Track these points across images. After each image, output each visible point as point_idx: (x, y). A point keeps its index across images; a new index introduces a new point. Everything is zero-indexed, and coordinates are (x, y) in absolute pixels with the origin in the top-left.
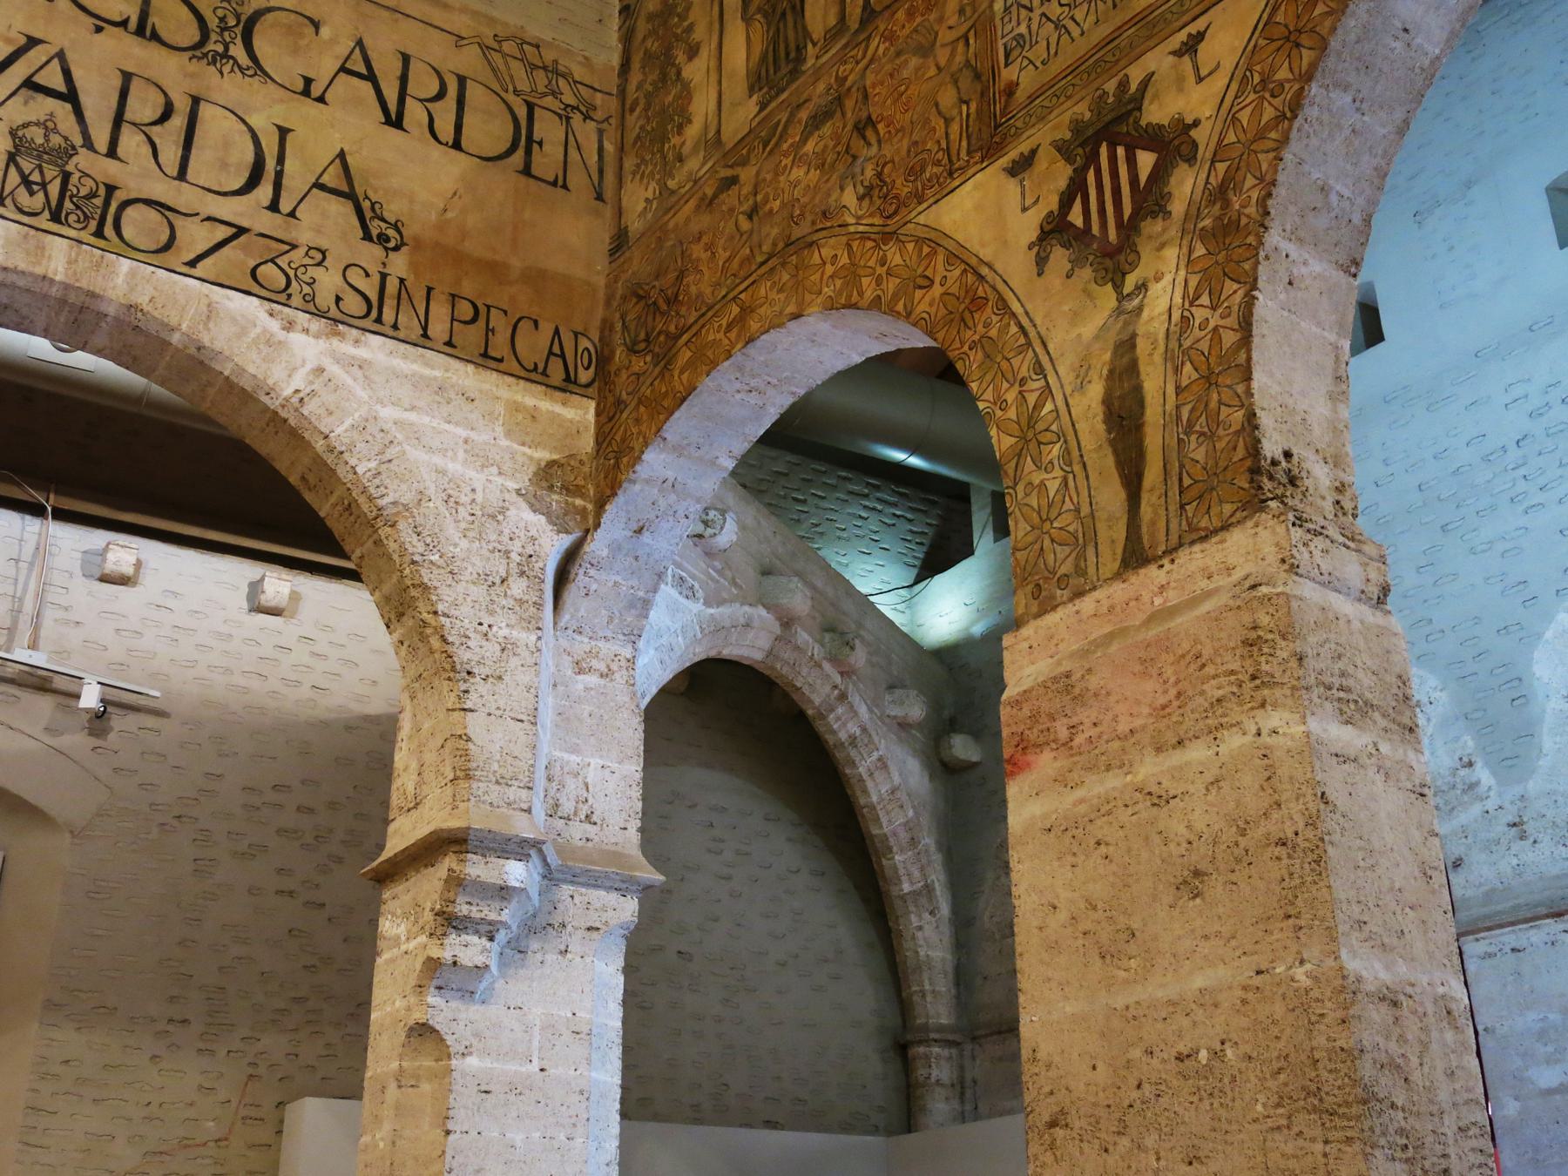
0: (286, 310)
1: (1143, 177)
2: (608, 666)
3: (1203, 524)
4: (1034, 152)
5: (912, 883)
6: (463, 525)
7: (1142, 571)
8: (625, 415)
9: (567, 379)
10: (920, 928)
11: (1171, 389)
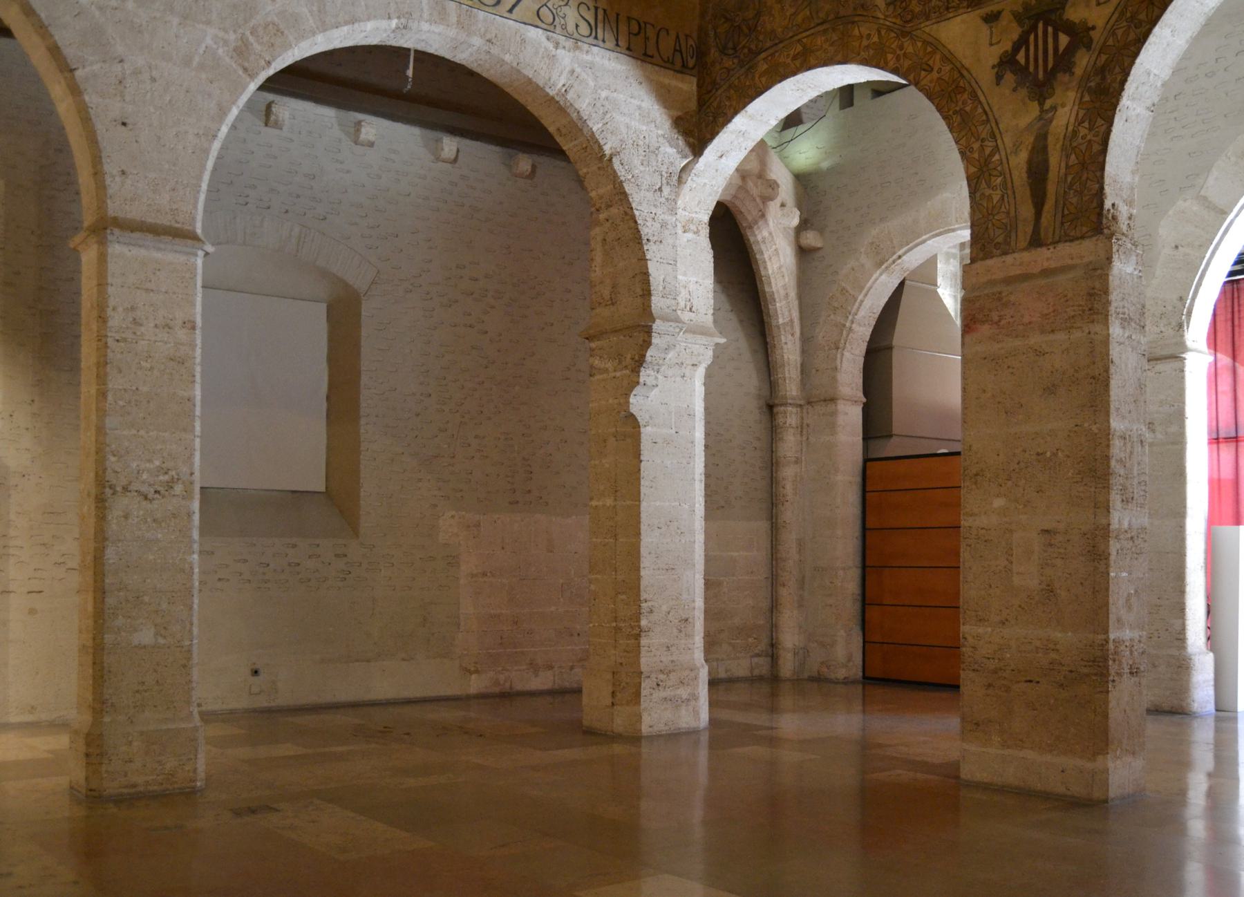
0: (555, 35)
1: (1061, 48)
2: (697, 228)
3: (1071, 234)
4: (999, 13)
5: (784, 319)
6: (641, 158)
7: (1039, 249)
8: (720, 92)
9: (683, 66)
10: (786, 343)
11: (1063, 165)
